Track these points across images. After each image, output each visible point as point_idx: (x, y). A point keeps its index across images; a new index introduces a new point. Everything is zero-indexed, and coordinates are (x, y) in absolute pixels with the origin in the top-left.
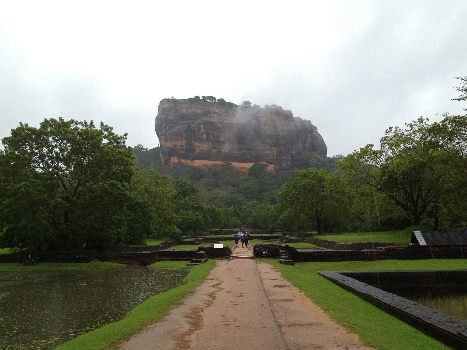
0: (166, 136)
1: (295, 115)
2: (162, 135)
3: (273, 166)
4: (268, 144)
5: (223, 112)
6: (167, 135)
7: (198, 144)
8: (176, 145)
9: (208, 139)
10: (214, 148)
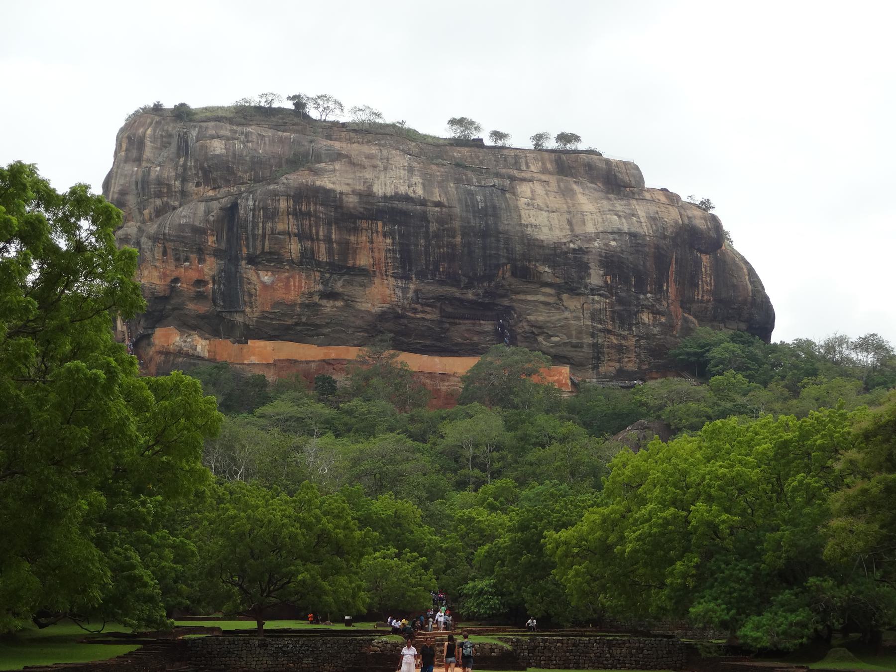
1: (651, 181)
3: (566, 370)
5: (369, 157)
6: (144, 240)
7: (266, 278)
8: (176, 280)
9: (307, 260)
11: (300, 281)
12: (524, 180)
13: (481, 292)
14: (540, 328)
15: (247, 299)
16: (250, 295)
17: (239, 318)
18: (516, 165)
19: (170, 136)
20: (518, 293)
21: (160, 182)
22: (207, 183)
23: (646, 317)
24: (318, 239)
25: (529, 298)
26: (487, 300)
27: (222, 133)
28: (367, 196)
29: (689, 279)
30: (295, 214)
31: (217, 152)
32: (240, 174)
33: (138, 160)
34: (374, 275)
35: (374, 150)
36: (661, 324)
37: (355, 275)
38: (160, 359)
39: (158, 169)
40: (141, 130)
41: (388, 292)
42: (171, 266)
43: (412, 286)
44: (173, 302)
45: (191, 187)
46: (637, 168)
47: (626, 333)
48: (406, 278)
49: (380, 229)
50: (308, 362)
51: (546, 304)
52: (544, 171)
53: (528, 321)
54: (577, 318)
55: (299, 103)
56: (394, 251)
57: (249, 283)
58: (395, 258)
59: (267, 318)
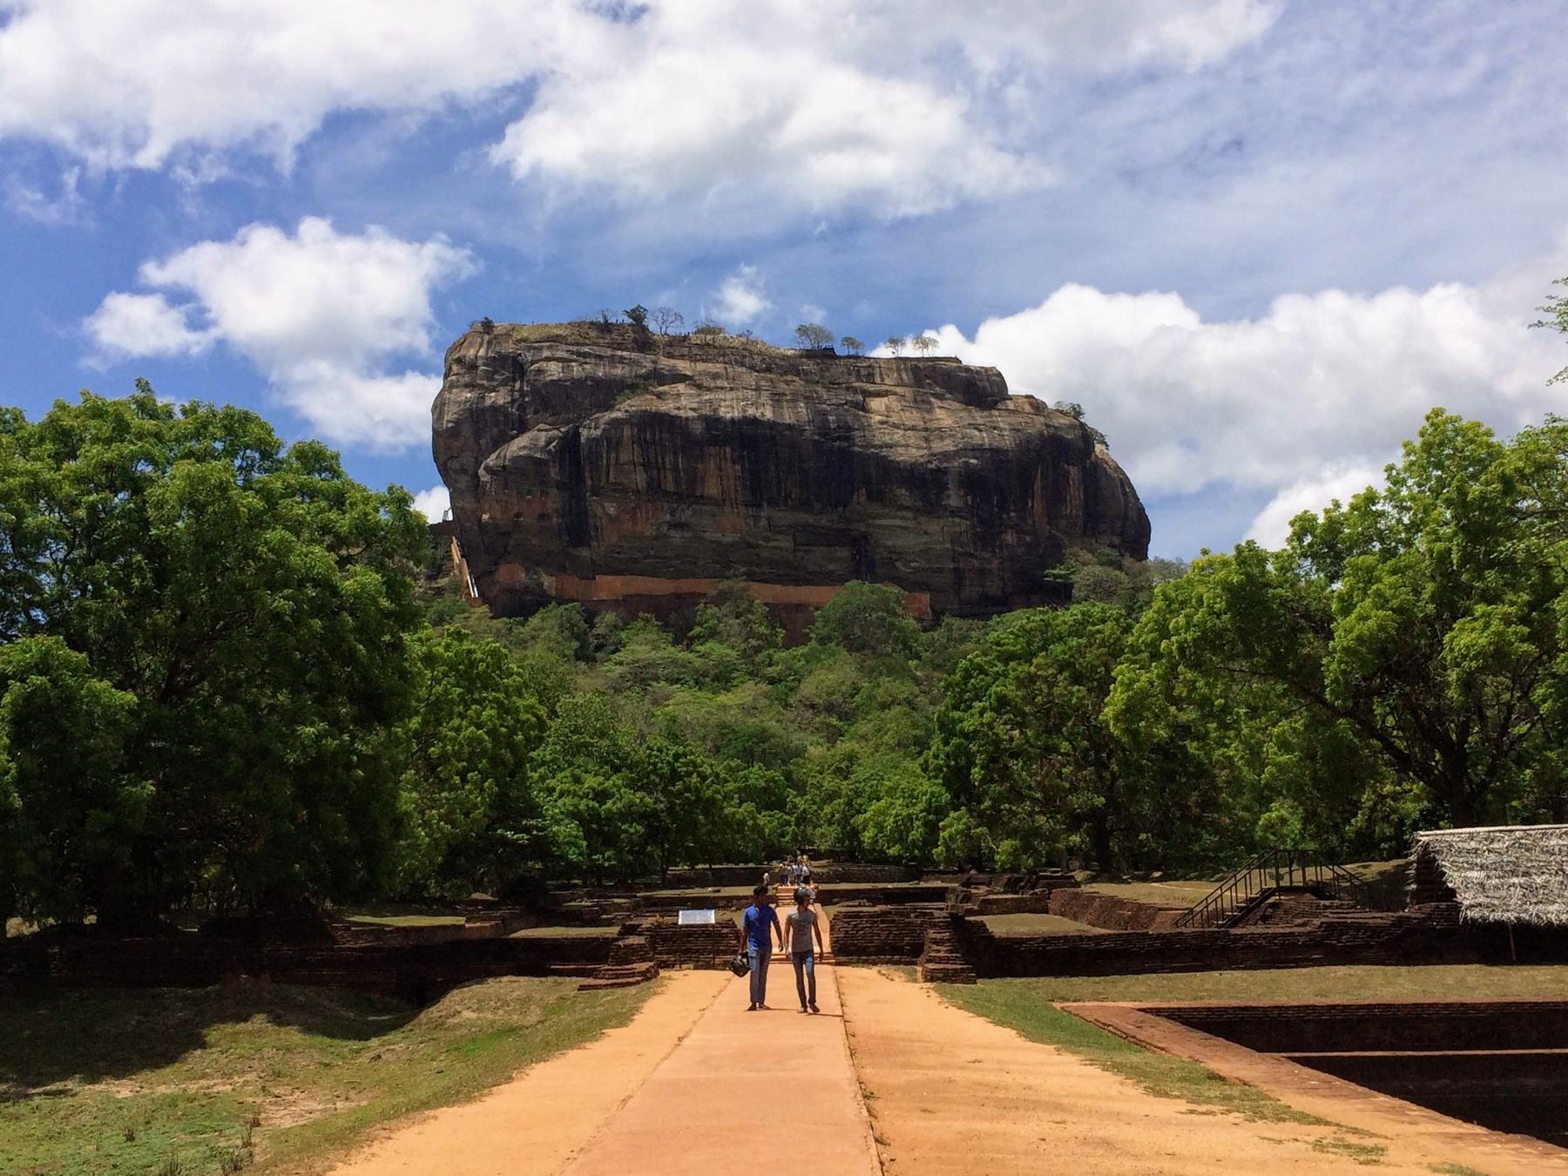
1: (1014, 387)
2: (464, 471)
3: (926, 597)
4: (907, 508)
5: (715, 376)
8: (518, 515)
12: (878, 394)
18: (870, 378)
21: (495, 409)
23: (1010, 538)
26: (841, 526)
28: (712, 422)
29: (1056, 496)
35: (718, 368)
36: (1028, 545)
40: (472, 352)
46: (999, 375)
47: (987, 555)
51: (905, 528)
54: (939, 543)
55: (637, 316)
58: (744, 487)
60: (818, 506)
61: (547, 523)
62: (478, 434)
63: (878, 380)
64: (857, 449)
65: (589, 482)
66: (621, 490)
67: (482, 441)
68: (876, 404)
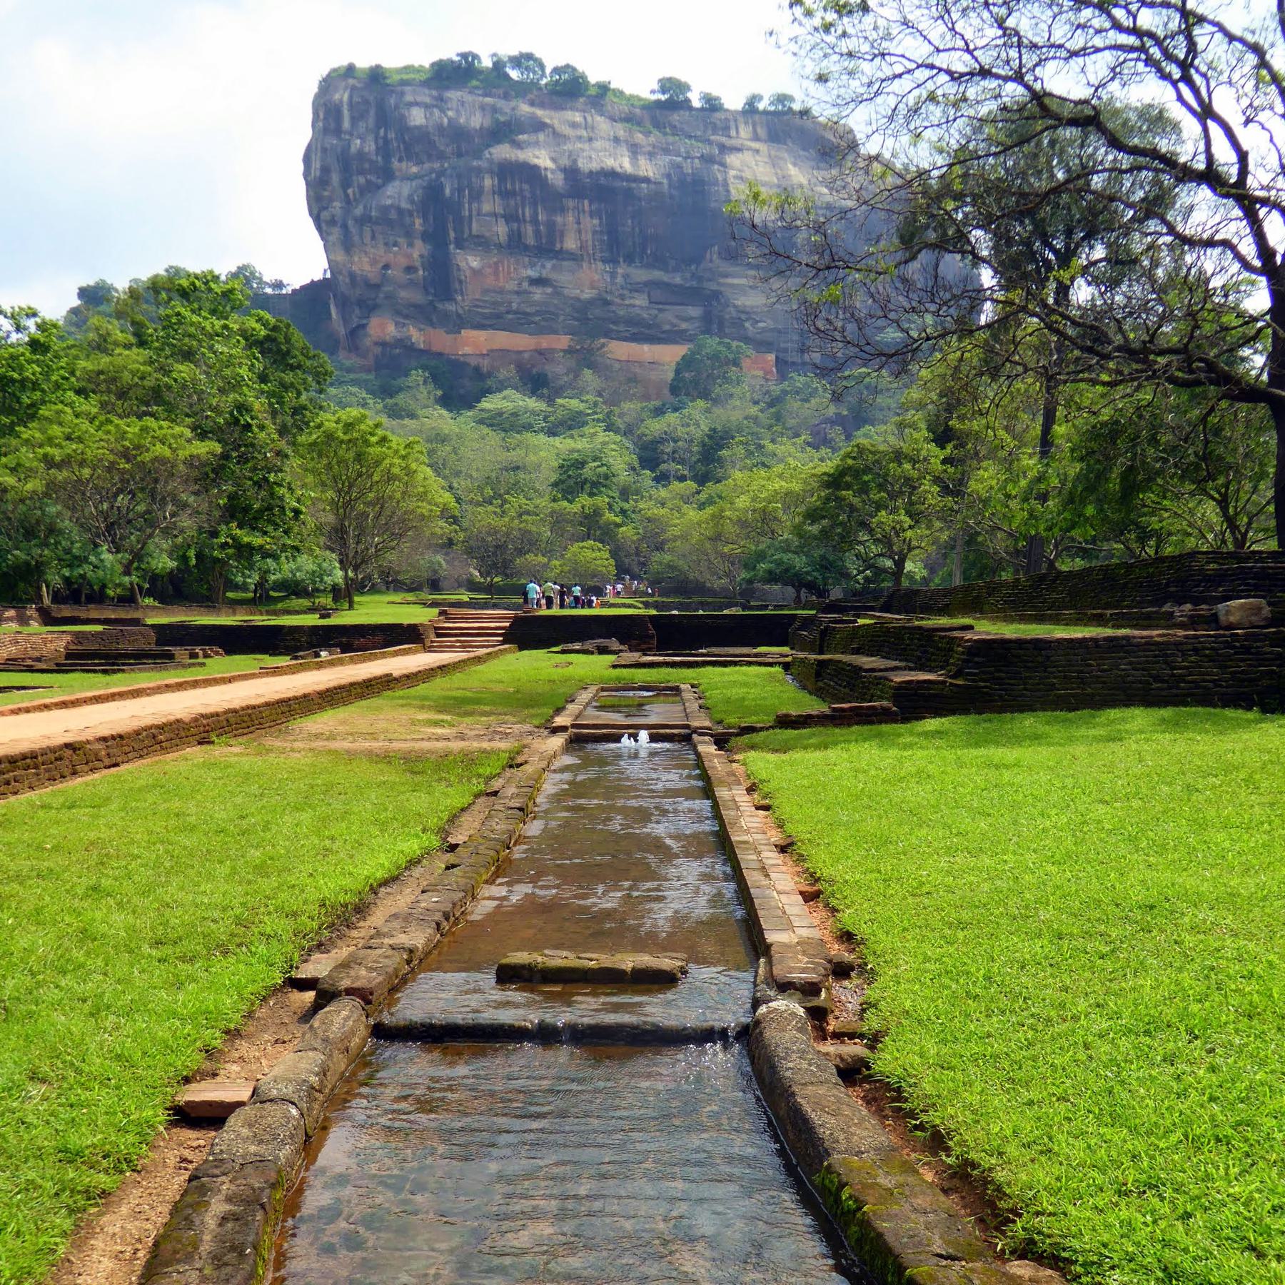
0: (345, 227)
2: (332, 222)
5: (574, 125)
6: (350, 223)
7: (475, 262)
8: (386, 267)
9: (515, 245)
10: (539, 282)
11: (509, 267)
13: (688, 275)
14: (748, 313)
15: (457, 286)
16: (461, 282)
17: (451, 307)
19: (366, 102)
20: (727, 276)
21: (361, 155)
22: (409, 158)
24: (525, 221)
25: (736, 281)
26: (694, 283)
27: (419, 99)
28: (571, 173)
30: (500, 193)
31: (418, 123)
32: (442, 148)
33: (338, 131)
34: (582, 260)
35: (578, 117)
37: (563, 259)
38: (378, 350)
39: (358, 141)
41: (597, 277)
42: (381, 251)
43: (620, 271)
44: (386, 289)
45: (395, 164)
48: (614, 261)
49: (587, 208)
50: (520, 352)
52: (756, 138)
53: (735, 306)
56: (601, 232)
57: (459, 269)
58: (602, 241)
59: (477, 306)
60: (672, 263)
61: (413, 276)
62: (346, 184)
63: (733, 133)
64: (713, 205)
65: (452, 234)
66: (482, 243)
67: (350, 191)
68: (732, 159)
